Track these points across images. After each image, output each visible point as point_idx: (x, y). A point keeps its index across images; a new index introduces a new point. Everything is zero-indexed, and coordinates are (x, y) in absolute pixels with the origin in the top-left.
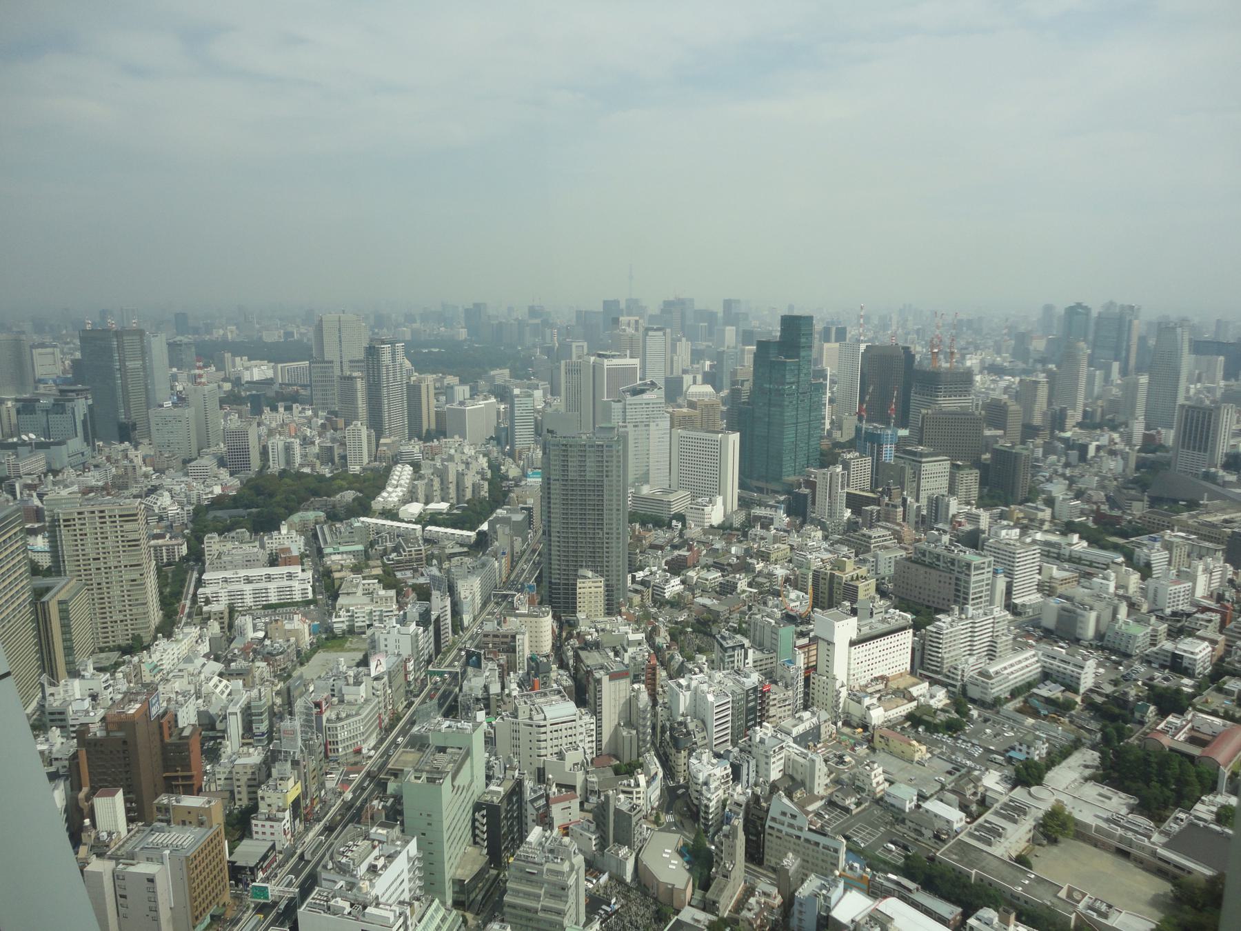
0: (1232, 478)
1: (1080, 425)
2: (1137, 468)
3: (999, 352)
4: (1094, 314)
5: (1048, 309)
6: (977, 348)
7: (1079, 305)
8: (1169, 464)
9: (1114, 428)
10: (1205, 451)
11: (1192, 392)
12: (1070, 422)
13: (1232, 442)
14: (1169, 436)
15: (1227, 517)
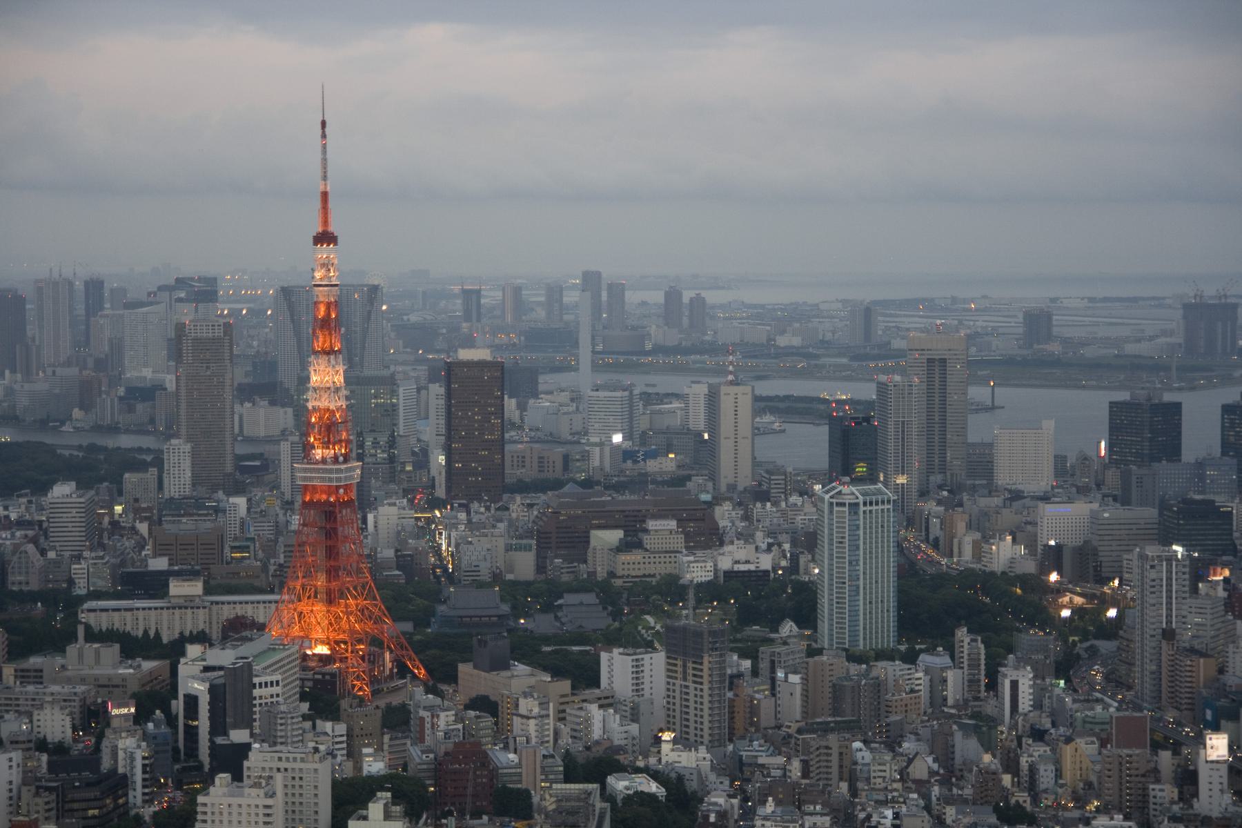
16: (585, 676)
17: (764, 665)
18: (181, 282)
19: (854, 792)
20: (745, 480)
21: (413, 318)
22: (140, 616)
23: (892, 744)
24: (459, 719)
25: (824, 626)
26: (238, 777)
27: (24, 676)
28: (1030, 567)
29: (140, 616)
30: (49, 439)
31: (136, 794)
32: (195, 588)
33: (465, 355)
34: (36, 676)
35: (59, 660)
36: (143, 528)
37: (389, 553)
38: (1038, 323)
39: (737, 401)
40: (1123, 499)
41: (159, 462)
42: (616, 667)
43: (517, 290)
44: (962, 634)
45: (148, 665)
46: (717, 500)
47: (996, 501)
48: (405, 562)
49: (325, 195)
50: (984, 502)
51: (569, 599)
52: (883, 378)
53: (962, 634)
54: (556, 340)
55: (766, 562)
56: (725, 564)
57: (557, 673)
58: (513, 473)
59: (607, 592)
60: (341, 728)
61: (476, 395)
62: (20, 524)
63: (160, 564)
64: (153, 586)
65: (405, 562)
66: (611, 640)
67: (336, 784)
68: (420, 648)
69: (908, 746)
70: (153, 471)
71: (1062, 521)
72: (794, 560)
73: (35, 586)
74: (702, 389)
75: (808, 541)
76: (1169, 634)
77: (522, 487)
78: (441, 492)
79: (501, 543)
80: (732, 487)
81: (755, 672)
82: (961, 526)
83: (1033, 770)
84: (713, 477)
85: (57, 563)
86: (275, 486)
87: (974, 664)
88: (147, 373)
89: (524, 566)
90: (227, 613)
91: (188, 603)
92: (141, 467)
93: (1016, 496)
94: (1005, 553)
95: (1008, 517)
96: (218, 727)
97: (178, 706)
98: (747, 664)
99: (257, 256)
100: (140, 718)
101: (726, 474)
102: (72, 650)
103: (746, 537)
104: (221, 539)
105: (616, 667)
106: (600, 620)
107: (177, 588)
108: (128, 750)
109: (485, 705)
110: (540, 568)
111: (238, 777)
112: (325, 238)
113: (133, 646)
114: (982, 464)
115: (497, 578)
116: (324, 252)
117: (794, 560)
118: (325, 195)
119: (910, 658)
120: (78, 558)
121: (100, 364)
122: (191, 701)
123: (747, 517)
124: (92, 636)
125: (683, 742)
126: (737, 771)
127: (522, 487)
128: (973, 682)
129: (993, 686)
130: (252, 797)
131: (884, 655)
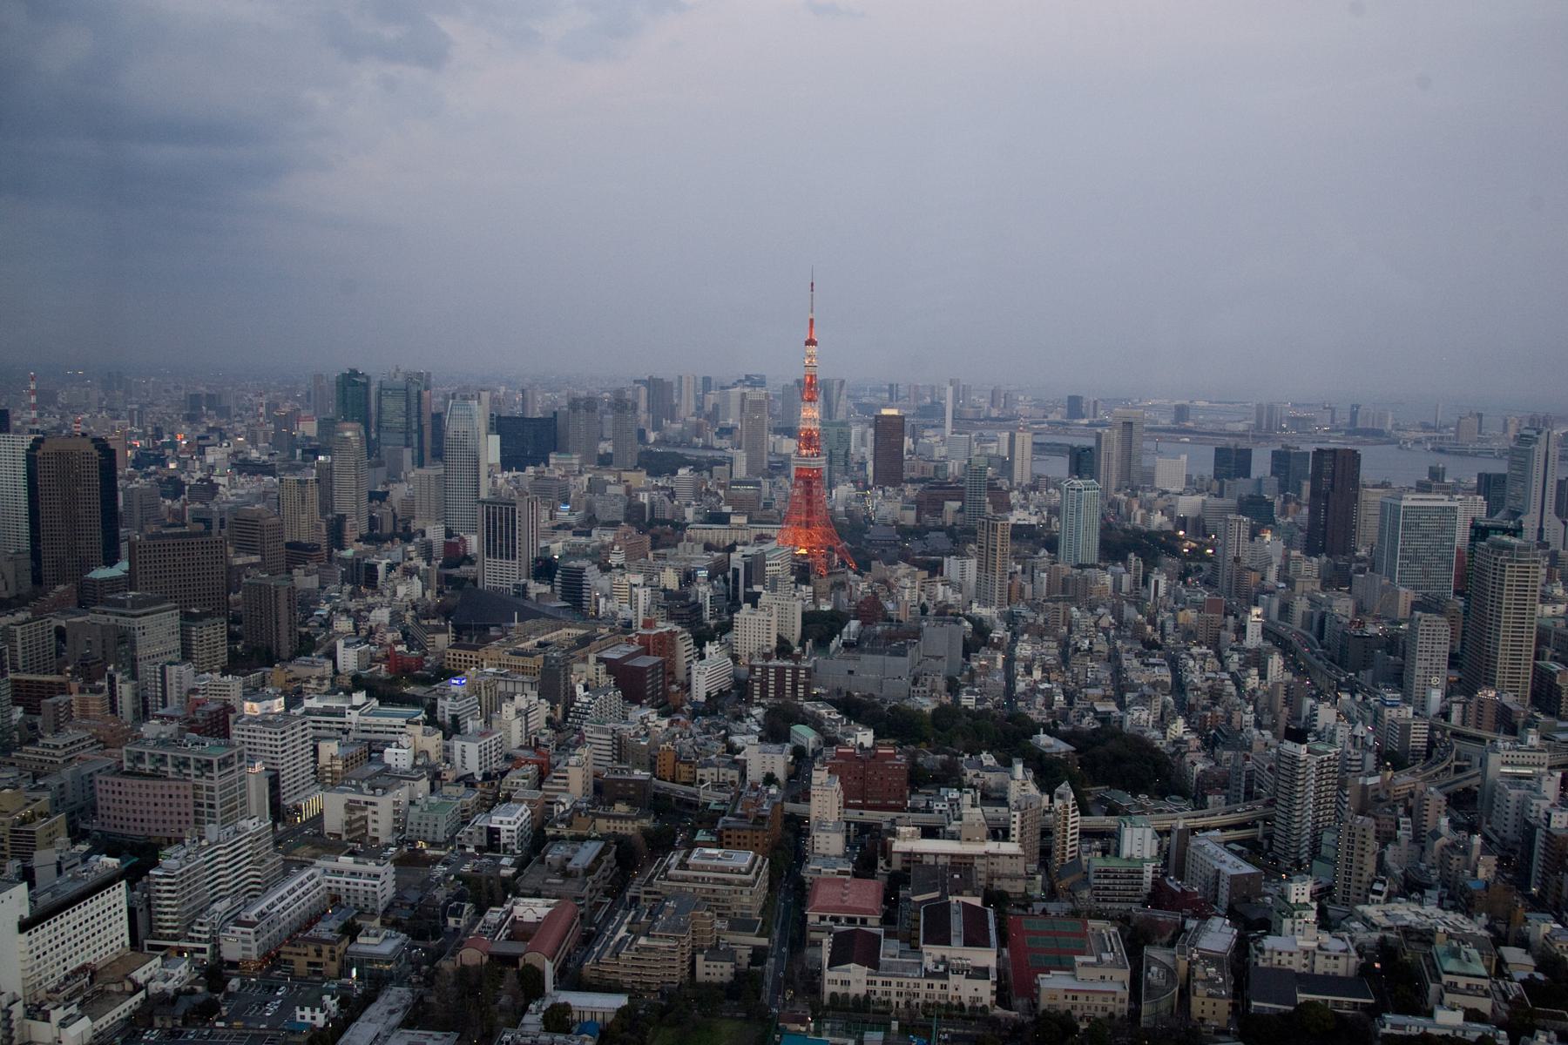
0: (546, 589)
1: (363, 539)
2: (440, 592)
3: (253, 441)
4: (374, 388)
5: (318, 377)
6: (223, 437)
7: (354, 373)
8: (475, 582)
9: (407, 537)
10: (514, 557)
11: (500, 482)
12: (350, 535)
13: (543, 544)
14: (473, 543)
15: (542, 639)
16: (935, 569)
17: (1028, 569)
18: (748, 377)
19: (1070, 631)
20: (1027, 481)
21: (864, 400)
22: (717, 534)
23: (1092, 609)
24: (870, 587)
25: (1061, 552)
26: (755, 605)
27: (657, 557)
28: (1170, 527)
29: (717, 534)
30: (679, 451)
31: (707, 614)
32: (744, 520)
33: (885, 412)
34: (664, 557)
35: (674, 551)
36: (721, 492)
37: (842, 509)
38: (1181, 412)
39: (1025, 441)
40: (1220, 495)
41: (731, 461)
42: (951, 565)
43: (916, 387)
44: (1132, 556)
45: (717, 555)
46: (1011, 489)
47: (1155, 495)
48: (849, 513)
49: (812, 321)
50: (1149, 495)
51: (932, 534)
52: (1099, 430)
53: (1132, 556)
54: (932, 413)
55: (1034, 520)
56: (1013, 520)
57: (922, 566)
58: (907, 475)
59: (950, 532)
60: (810, 589)
61: (889, 433)
62: (663, 488)
63: (727, 509)
64: (722, 519)
65: (849, 513)
66: (949, 555)
67: (804, 614)
68: (853, 553)
69: (1100, 611)
70: (727, 467)
71: (1188, 505)
72: (1049, 520)
73: (667, 517)
74: (1006, 434)
75: (1055, 511)
76: (1237, 560)
77: (912, 481)
78: (870, 483)
79: (899, 506)
80: (1019, 484)
81: (1024, 572)
82: (1136, 507)
83: (1163, 623)
84: (1011, 480)
85: (679, 507)
86: (788, 476)
87: (1137, 569)
88: (730, 421)
89: (910, 518)
90: (758, 532)
91: (740, 527)
92: (723, 464)
93: (1167, 492)
94: (1158, 520)
95: (1161, 502)
96: (748, 584)
97: (730, 575)
98: (1019, 567)
99: (783, 364)
100: (710, 578)
101: (1017, 478)
102: (680, 545)
103: (1025, 507)
104: (759, 498)
105: (951, 565)
106: (947, 544)
107: (733, 520)
108: (704, 592)
109: (885, 582)
110: (918, 519)
111: (755, 605)
112: (811, 342)
113: (708, 547)
114: (1149, 477)
115: (895, 522)
116: (811, 349)
117: (1049, 520)
118: (812, 321)
119: (1105, 569)
120: (688, 505)
121: (708, 417)
122: (736, 571)
123: (1026, 498)
124: (689, 540)
125: (985, 603)
126: (1011, 619)
127: (912, 481)
128: (1136, 582)
129: (1146, 582)
130: (761, 615)
131: (1093, 566)
